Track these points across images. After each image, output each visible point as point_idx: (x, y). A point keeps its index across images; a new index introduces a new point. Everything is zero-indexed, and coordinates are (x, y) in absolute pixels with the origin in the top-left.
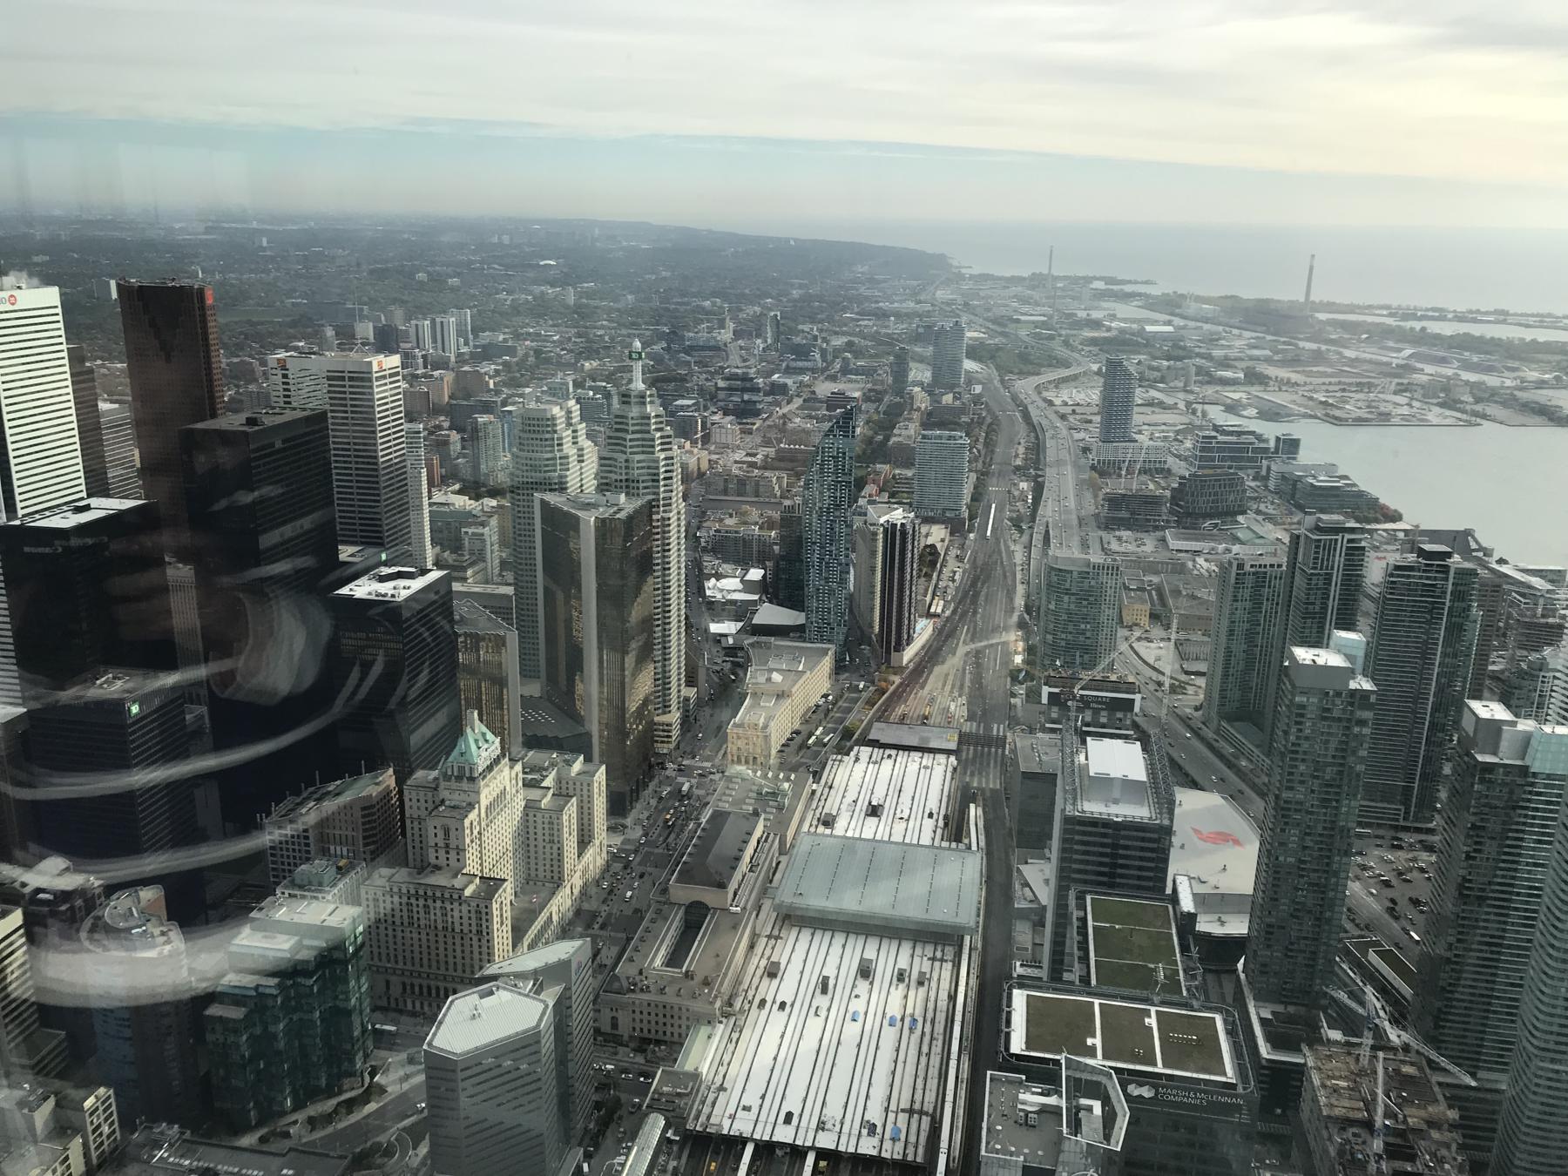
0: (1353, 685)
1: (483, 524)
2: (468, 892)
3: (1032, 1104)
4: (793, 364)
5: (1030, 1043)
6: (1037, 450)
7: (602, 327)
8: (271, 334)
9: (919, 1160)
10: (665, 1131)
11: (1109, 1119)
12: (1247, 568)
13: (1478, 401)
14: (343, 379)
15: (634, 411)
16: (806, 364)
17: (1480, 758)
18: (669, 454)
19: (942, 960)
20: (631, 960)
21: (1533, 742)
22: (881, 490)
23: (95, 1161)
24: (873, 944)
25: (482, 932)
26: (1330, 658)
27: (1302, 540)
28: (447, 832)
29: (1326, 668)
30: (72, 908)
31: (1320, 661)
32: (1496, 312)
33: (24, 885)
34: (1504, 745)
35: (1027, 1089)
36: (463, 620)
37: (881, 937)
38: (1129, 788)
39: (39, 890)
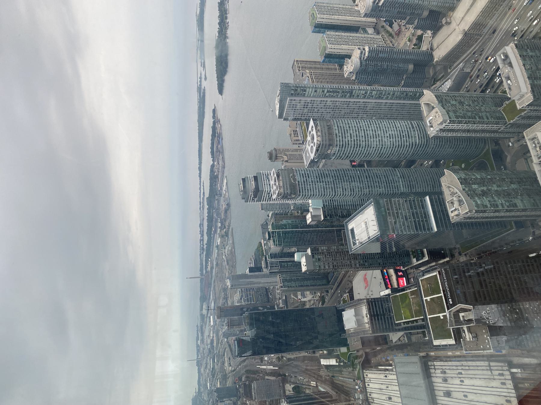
0: (310, 254)
3: (469, 336)
5: (450, 337)
11: (465, 310)
12: (282, 285)
13: (225, 227)
17: (322, 218)
19: (434, 366)
21: (315, 207)
24: (437, 393)
26: (303, 261)
27: (271, 271)
29: (306, 262)
31: (305, 264)
32: (200, 242)
34: (318, 214)
35: (465, 337)
37: (434, 390)
38: (357, 314)
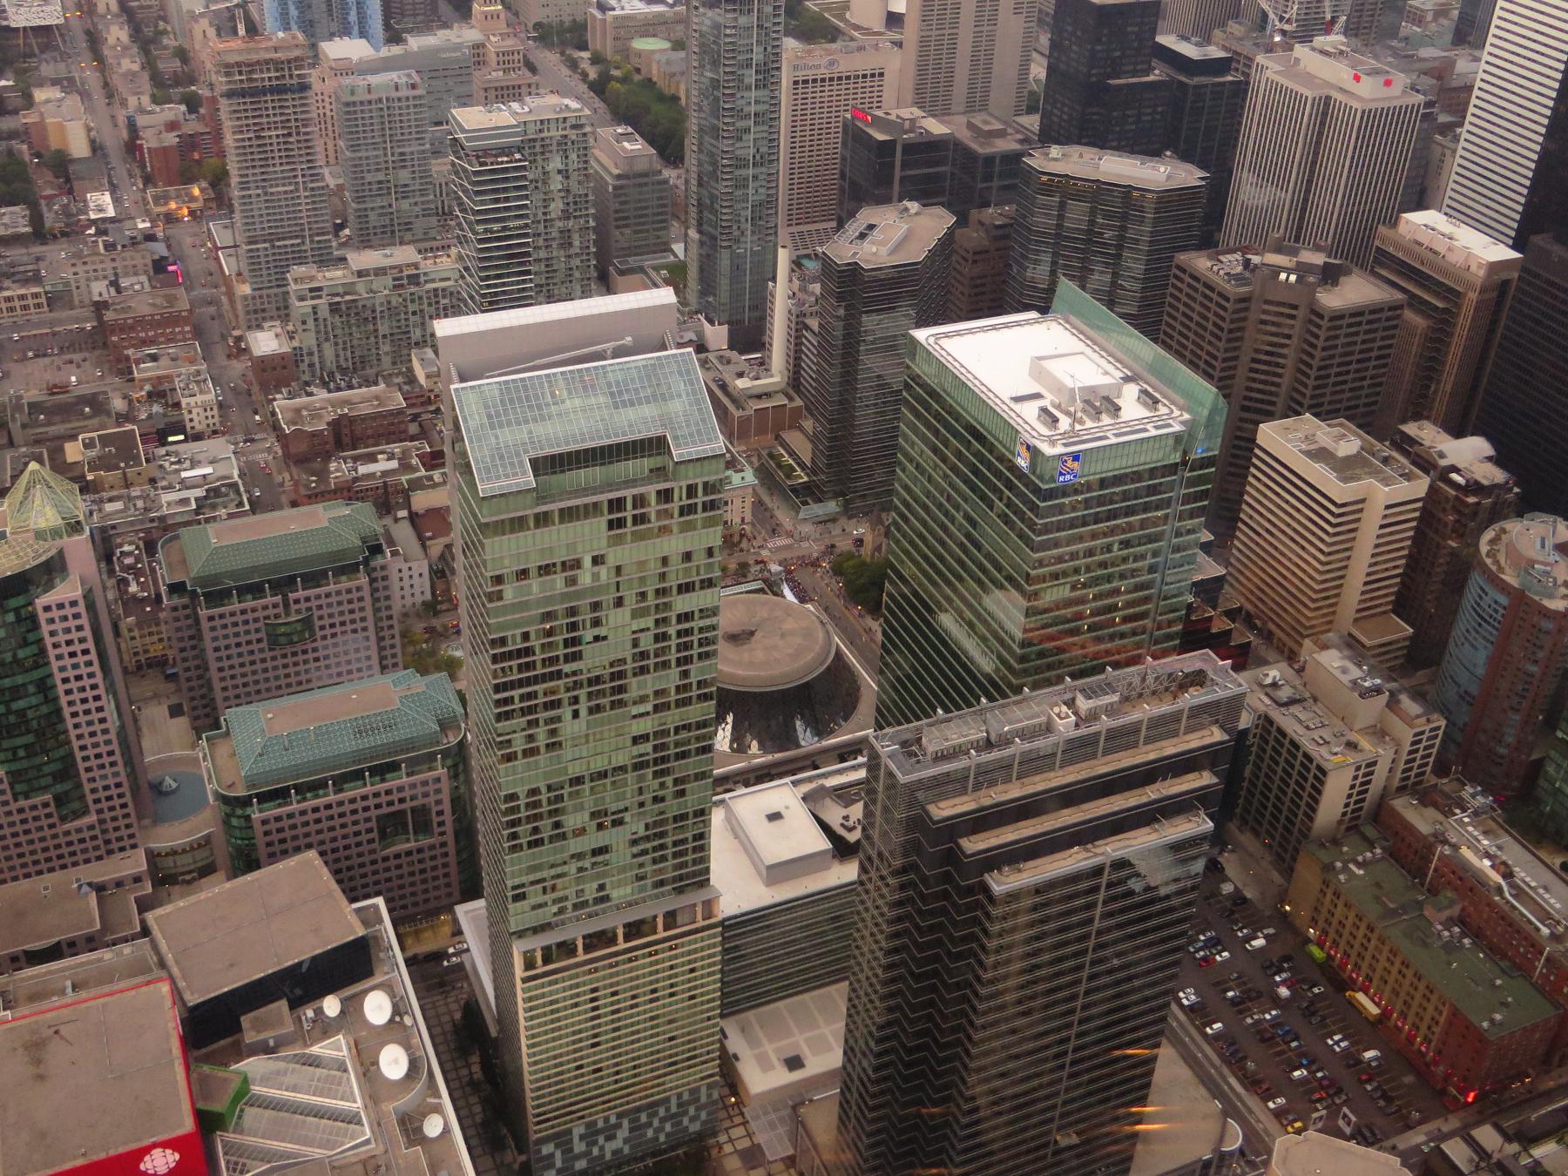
23: (1396, 783)
30: (1478, 504)
33: (1442, 455)
39: (1457, 470)
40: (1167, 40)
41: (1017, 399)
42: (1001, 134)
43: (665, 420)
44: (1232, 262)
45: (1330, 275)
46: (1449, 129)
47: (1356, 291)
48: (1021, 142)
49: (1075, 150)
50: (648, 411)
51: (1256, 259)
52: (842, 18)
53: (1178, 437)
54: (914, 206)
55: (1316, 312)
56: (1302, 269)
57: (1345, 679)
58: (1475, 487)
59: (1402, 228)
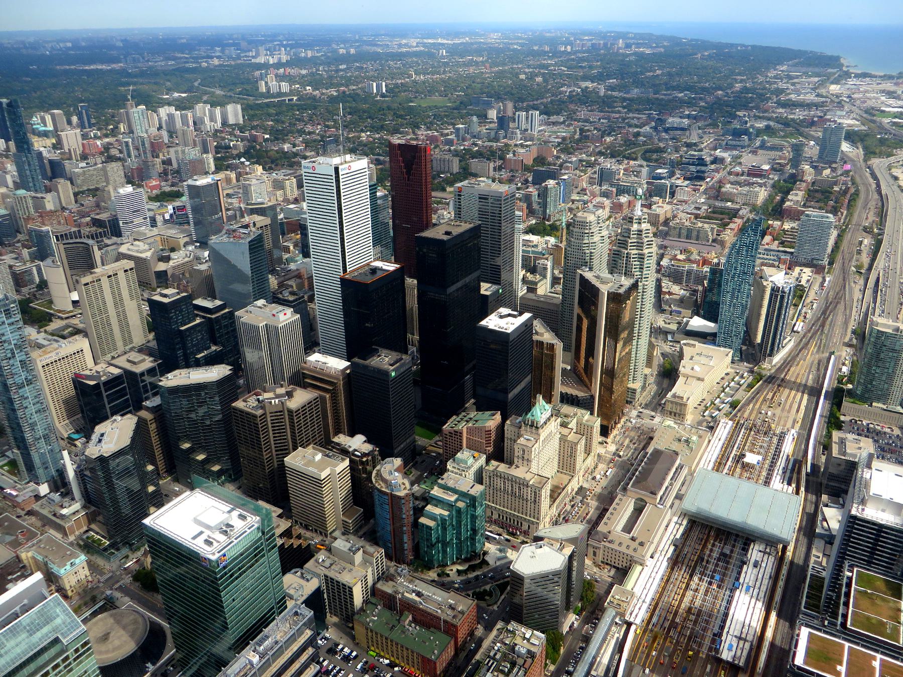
1: (547, 259)
2: (531, 483)
4: (731, 142)
5: (805, 663)
6: (882, 214)
7: (619, 112)
8: (446, 116)
9: (741, 664)
10: (615, 617)
14: (487, 199)
15: (635, 227)
16: (738, 143)
18: (650, 250)
19: (769, 554)
20: (606, 524)
22: (774, 240)
25: (536, 501)
28: (524, 451)
36: (537, 333)
39: (356, 450)
40: (199, 302)
41: (194, 538)
42: (143, 360)
43: (55, 630)
44: (252, 402)
45: (290, 395)
46: (311, 299)
47: (301, 398)
48: (151, 362)
49: (177, 372)
50: (45, 630)
51: (261, 398)
52: (51, 309)
53: (258, 528)
54: (118, 418)
55: (290, 412)
56: (277, 396)
57: (346, 549)
58: (364, 455)
59: (308, 364)
